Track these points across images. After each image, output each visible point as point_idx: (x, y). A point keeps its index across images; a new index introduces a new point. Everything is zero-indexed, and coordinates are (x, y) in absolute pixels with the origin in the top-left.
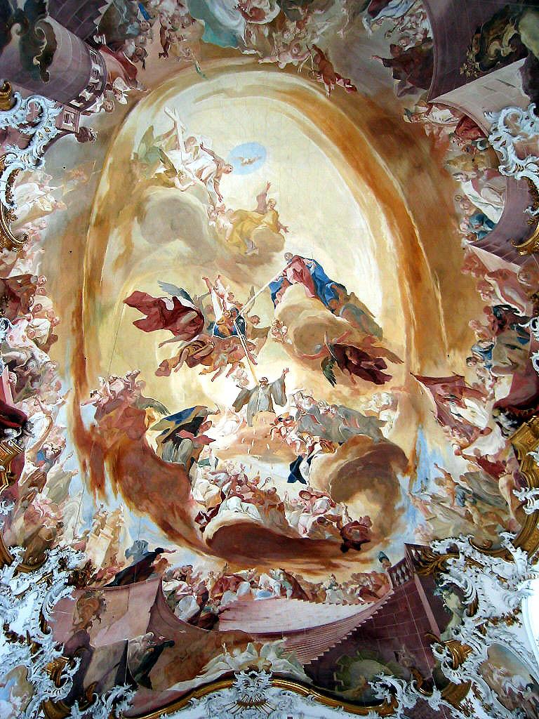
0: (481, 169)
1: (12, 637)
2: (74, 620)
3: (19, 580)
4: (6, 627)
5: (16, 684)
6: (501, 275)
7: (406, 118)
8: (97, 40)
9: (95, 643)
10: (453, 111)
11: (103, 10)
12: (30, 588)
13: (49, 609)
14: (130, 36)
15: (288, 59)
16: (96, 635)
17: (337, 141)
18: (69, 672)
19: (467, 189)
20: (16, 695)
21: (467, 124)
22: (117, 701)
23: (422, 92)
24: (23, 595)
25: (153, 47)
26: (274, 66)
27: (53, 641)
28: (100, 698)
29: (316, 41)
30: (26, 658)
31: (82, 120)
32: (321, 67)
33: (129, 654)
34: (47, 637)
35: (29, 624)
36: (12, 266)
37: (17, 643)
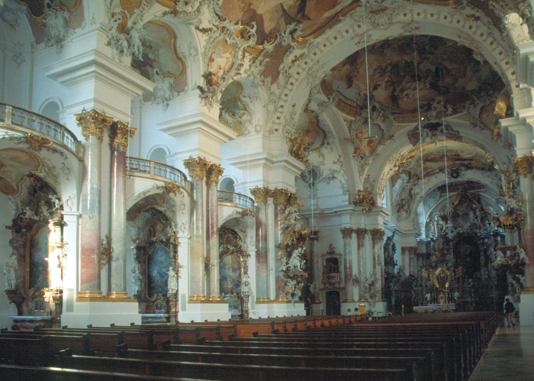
1: (204, 31)
2: (239, 6)
3: (191, 4)
4: (197, 28)
5: (222, 49)
9: (260, 11)
12: (201, 4)
13: (219, 9)
16: (258, 7)
18: (251, 30)
20: (225, 53)
22: (292, 33)
24: (198, 10)
27: (230, 22)
28: (281, 34)
30: (220, 35)
33: (286, 8)
34: (225, 22)
35: (212, 20)
37: (209, 32)
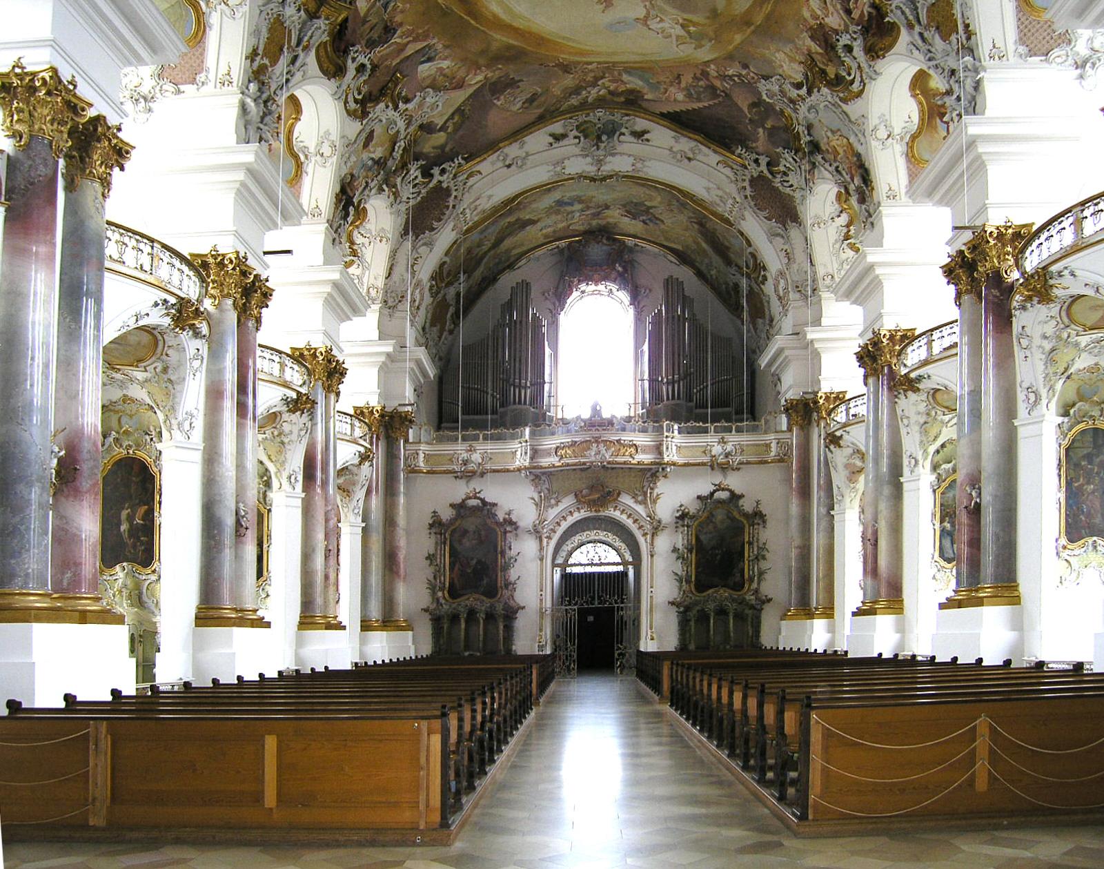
0: (441, 77)
6: (402, 48)
7: (500, 66)
8: (722, 94)
10: (470, 85)
11: (716, 101)
14: (701, 87)
15: (590, 67)
17: (549, 41)
19: (445, 64)
21: (460, 85)
23: (494, 80)
25: (687, 79)
26: (599, 63)
29: (572, 76)
31: (744, 72)
32: (566, 68)
36: (817, 53)
